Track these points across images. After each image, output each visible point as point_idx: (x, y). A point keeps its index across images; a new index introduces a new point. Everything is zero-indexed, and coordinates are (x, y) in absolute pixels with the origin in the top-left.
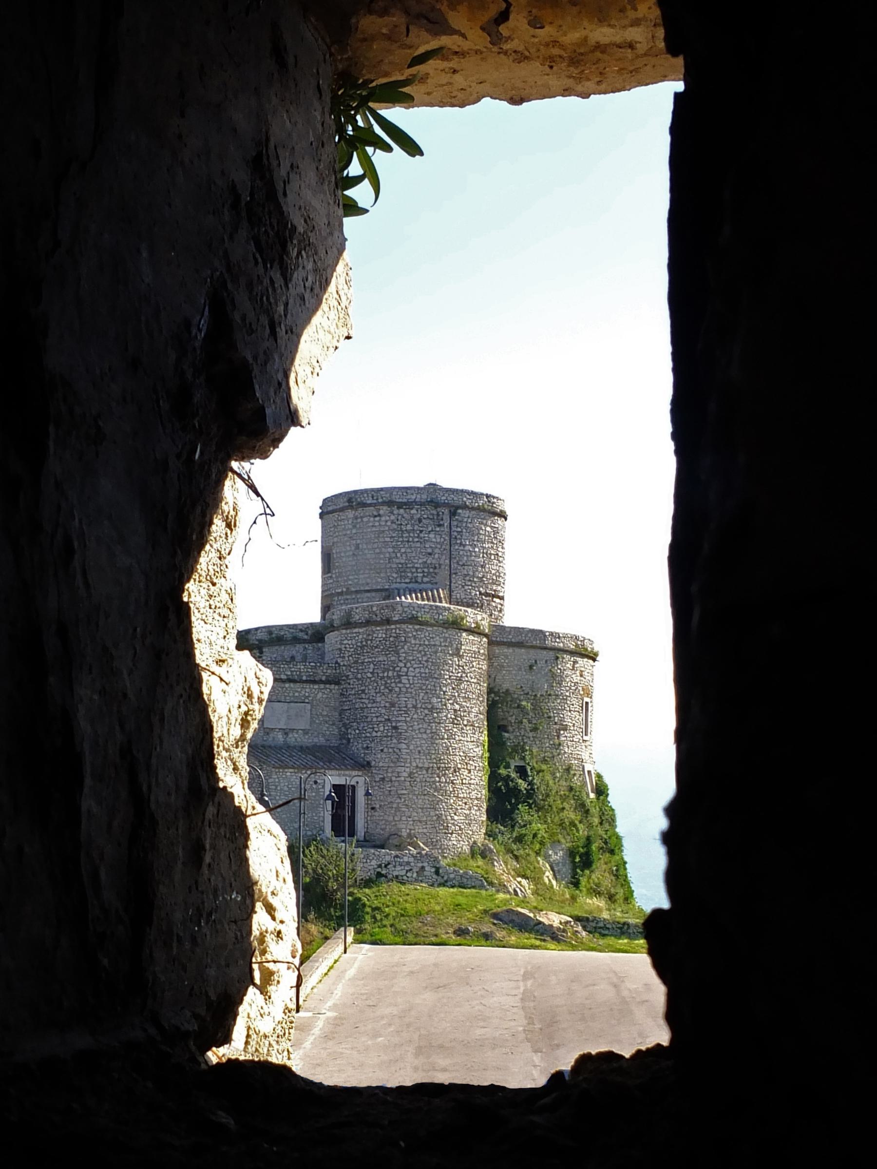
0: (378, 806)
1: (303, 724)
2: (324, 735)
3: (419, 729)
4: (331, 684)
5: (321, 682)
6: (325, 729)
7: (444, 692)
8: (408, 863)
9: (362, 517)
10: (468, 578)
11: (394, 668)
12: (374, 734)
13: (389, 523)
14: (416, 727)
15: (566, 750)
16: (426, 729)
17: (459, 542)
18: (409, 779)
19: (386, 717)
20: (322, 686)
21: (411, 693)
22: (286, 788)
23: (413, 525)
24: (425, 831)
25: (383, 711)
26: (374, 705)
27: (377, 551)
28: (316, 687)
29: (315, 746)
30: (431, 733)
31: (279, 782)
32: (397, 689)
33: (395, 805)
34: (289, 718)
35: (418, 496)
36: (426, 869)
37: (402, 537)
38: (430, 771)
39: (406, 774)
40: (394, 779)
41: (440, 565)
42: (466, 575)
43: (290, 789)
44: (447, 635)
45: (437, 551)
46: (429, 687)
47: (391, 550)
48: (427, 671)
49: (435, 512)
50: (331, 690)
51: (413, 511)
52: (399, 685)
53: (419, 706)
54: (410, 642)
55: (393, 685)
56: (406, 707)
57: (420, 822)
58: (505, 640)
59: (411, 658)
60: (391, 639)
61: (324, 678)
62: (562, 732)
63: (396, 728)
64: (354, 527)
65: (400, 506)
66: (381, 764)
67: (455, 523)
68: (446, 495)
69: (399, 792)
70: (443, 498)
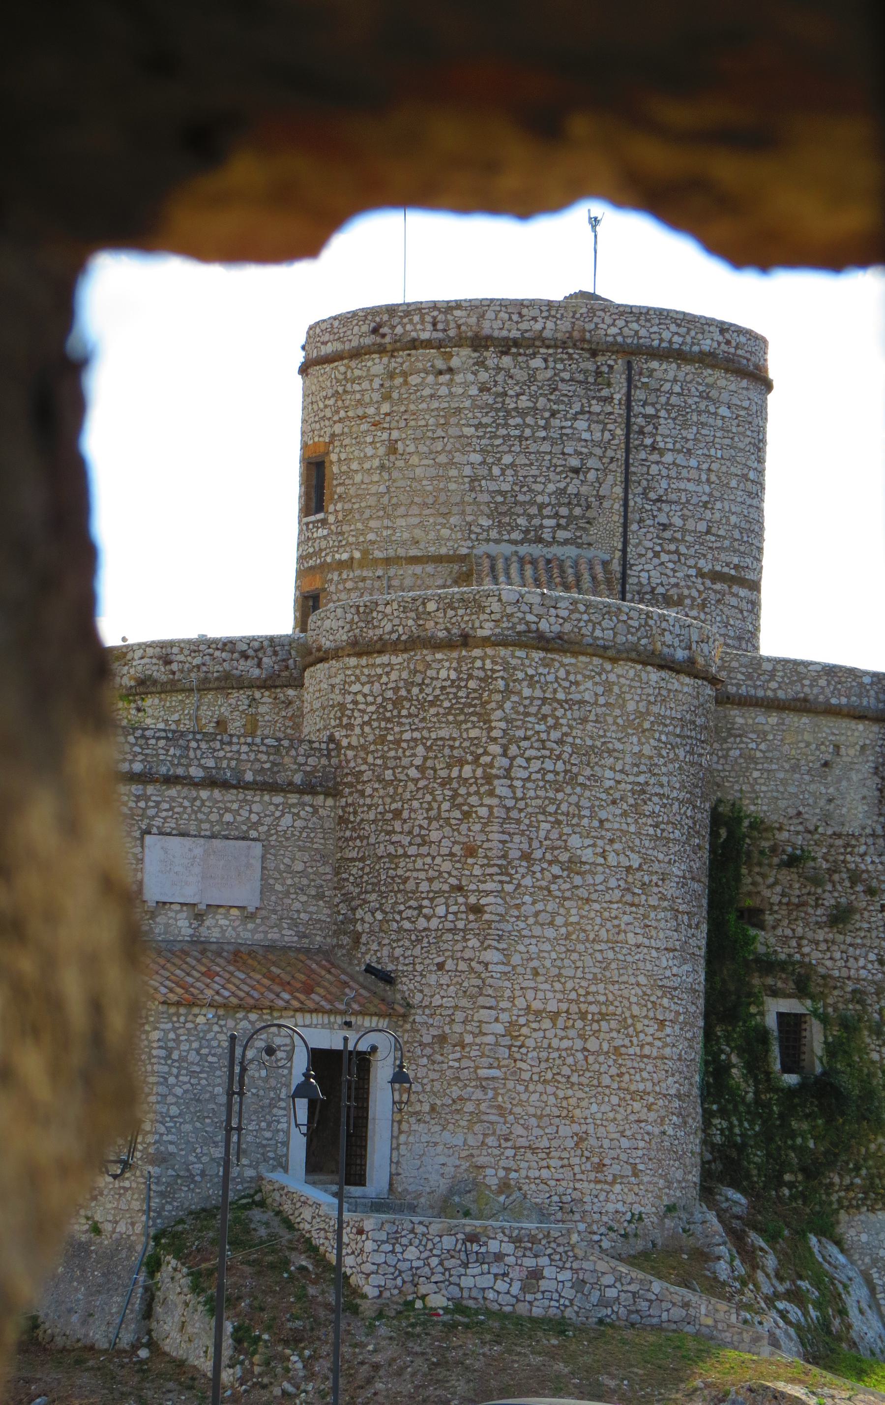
0: (426, 1108)
1: (246, 893)
2: (294, 924)
3: (537, 914)
4: (314, 793)
5: (288, 788)
6: (297, 905)
7: (601, 822)
8: (499, 1257)
9: (405, 374)
10: (667, 534)
11: (477, 758)
12: (422, 923)
13: (473, 391)
14: (528, 909)
17: (648, 441)
18: (506, 1041)
19: (453, 881)
20: (293, 799)
21: (518, 822)
22: (193, 1057)
23: (534, 397)
24: (545, 1173)
25: (447, 866)
26: (424, 850)
27: (442, 459)
28: (278, 799)
29: (271, 948)
30: (566, 924)
31: (177, 1040)
32: (483, 812)
33: (470, 1107)
35: (550, 325)
36: (546, 1273)
37: (506, 425)
38: (560, 1023)
39: (499, 1028)
40: (468, 1039)
41: (600, 498)
42: (665, 527)
43: (203, 1058)
44: (612, 678)
45: (591, 463)
47: (476, 458)
48: (560, 766)
49: (590, 366)
50: (316, 811)
52: (487, 801)
53: (538, 854)
54: (519, 693)
55: (473, 800)
56: (504, 857)
57: (534, 1150)
58: (760, 693)
59: (521, 733)
60: (472, 684)
61: (298, 779)
63: (477, 910)
64: (386, 397)
66: (437, 1001)
68: (620, 323)
69: (482, 1073)
70: (613, 331)
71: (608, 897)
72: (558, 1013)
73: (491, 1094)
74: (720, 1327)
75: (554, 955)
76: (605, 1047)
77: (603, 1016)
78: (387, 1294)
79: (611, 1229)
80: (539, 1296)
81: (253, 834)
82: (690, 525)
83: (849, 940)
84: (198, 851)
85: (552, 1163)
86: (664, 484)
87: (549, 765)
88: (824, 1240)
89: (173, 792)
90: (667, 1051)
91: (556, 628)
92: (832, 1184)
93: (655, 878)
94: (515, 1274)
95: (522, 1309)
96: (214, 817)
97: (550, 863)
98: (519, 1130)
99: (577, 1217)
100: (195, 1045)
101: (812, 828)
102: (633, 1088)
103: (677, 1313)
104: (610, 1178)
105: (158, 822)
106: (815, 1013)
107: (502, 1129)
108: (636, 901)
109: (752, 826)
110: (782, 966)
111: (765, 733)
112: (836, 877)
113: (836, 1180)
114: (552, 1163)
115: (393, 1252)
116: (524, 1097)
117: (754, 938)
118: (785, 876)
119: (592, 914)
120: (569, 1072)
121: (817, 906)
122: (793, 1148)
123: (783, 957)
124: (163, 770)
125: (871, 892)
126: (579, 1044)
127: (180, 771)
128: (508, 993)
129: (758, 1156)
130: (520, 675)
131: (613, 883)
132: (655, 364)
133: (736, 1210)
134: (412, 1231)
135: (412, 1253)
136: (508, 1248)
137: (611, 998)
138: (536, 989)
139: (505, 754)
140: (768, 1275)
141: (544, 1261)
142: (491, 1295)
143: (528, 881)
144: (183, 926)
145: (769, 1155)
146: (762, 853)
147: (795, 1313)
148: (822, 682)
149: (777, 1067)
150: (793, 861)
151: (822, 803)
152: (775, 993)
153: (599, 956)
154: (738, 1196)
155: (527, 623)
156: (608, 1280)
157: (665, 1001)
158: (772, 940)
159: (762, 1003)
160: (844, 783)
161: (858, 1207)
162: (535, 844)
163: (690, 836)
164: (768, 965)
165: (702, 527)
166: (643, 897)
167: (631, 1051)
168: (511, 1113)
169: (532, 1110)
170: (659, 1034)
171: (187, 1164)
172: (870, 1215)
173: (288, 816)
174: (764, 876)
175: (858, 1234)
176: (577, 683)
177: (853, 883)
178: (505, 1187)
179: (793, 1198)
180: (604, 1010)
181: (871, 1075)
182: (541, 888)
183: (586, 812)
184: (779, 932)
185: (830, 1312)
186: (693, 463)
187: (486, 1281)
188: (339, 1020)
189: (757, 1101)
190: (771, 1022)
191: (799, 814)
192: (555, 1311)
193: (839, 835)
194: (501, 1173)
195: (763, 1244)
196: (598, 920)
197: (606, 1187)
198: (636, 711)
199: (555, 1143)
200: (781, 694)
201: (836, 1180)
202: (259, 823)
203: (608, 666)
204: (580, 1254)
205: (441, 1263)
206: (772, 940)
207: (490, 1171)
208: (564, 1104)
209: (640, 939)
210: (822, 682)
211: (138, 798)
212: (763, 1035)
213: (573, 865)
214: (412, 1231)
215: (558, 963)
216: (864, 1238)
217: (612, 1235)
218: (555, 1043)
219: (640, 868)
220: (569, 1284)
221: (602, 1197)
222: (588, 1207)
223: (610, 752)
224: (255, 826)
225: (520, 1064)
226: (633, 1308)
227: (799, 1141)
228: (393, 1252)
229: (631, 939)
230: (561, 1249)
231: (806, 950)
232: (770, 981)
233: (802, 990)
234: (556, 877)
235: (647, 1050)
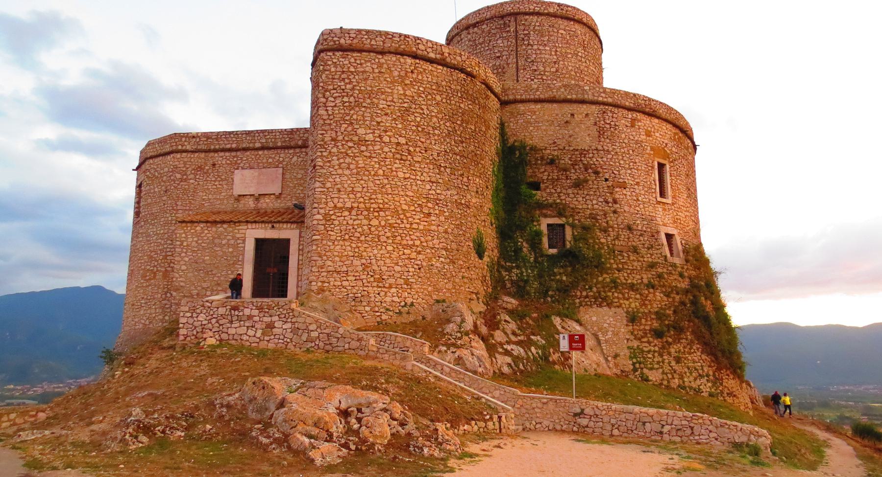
1: (276, 189)
6: (299, 191)
7: (378, 123)
8: (250, 317)
10: (537, 73)
15: (626, 208)
16: (349, 164)
17: (526, 42)
18: (323, 222)
20: (298, 150)
21: (330, 124)
22: (194, 244)
24: (345, 283)
28: (291, 151)
30: (357, 168)
31: (186, 237)
36: (276, 325)
38: (354, 212)
43: (199, 244)
44: (382, 61)
46: (355, 117)
48: (352, 99)
49: (502, 22)
51: (485, 26)
53: (340, 138)
54: (329, 70)
56: (323, 140)
58: (532, 97)
59: (331, 87)
61: (300, 143)
62: (617, 189)
65: (474, 25)
67: (522, 27)
71: (383, 156)
72: (352, 208)
73: (314, 247)
74: (381, 351)
75: (349, 182)
76: (383, 223)
77: (381, 209)
78: (188, 339)
79: (387, 309)
80: (272, 337)
81: (281, 165)
82: (548, 69)
83: (586, 193)
84: (256, 174)
85: (349, 278)
86: (534, 56)
87: (346, 99)
88: (567, 320)
89: (248, 153)
90: (433, 228)
91: (349, 42)
92: (576, 296)
93: (418, 149)
95: (263, 345)
96: (265, 161)
97: (347, 141)
98: (329, 263)
99: (364, 304)
100: (195, 239)
101: (561, 147)
102: (404, 242)
103: (354, 344)
104: (387, 285)
105: (242, 165)
106: (568, 223)
107: (320, 263)
108: (404, 158)
109: (531, 149)
110: (551, 206)
111: (535, 112)
112: (577, 167)
113: (579, 293)
114: (349, 278)
115: (192, 317)
116: (332, 247)
117: (535, 195)
118: (549, 168)
119: (373, 163)
120: (359, 235)
121: (567, 179)
122: (552, 280)
123: (550, 201)
124: (244, 146)
125: (597, 173)
126: (365, 222)
127: (251, 145)
128: (324, 200)
129: (536, 285)
130: (330, 63)
131: (386, 149)
132: (527, 17)
133: (509, 306)
134: (203, 306)
135: (202, 317)
137: (386, 201)
138: (339, 198)
139: (324, 97)
140: (506, 333)
141: (276, 318)
142: (245, 338)
143: (335, 150)
144: (251, 203)
145: (540, 284)
146: (537, 160)
147: (518, 350)
148: (562, 90)
149: (546, 246)
150: (552, 162)
151: (567, 137)
152: (546, 216)
153: (378, 182)
154: (513, 301)
155: (335, 41)
157: (430, 205)
158: (545, 195)
159: (538, 221)
160: (577, 129)
161: (591, 306)
162: (339, 134)
163: (449, 135)
164: (540, 206)
165: (553, 70)
166: (409, 157)
167: (402, 226)
168: (325, 255)
169: (336, 254)
170: (426, 219)
171: (190, 291)
172: (599, 309)
174: (539, 169)
175: (590, 317)
176: (361, 64)
177: (586, 170)
178: (321, 290)
179: (553, 302)
180: (381, 206)
181: (600, 248)
182: (342, 153)
183: (369, 119)
184: (548, 191)
185: (551, 350)
186: (547, 48)
187: (243, 330)
188: (270, 225)
189: (536, 260)
190: (544, 228)
191: (555, 143)
192: (281, 345)
193: (577, 150)
194: (320, 284)
195: (507, 318)
196: (377, 166)
197: (386, 290)
198: (399, 76)
199: (350, 269)
200: (542, 96)
201: (579, 293)
202: (283, 161)
203: (380, 57)
204: (296, 314)
205: (217, 322)
206: (545, 195)
207: (314, 283)
208: (357, 250)
209: (407, 175)
210: (562, 90)
211: (234, 157)
212: (539, 234)
213: (362, 142)
214: (203, 306)
215: (352, 185)
216: (594, 319)
217: (391, 313)
218: (350, 222)
219: (407, 144)
220: (289, 330)
221: (382, 294)
222: (372, 299)
223: (383, 93)
224: (281, 163)
225: (330, 233)
226: (328, 342)
227: (558, 277)
228: (192, 317)
229: (401, 175)
230: (285, 312)
231: (563, 198)
232: (544, 211)
233: (560, 215)
234: (350, 147)
235: (415, 226)
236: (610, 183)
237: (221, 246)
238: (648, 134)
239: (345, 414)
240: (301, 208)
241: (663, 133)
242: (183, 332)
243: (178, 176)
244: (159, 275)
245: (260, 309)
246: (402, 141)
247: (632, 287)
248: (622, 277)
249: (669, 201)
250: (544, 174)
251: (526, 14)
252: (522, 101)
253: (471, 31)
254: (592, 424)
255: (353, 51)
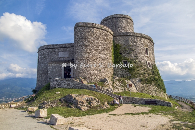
1: (67, 56)
5: (71, 47)
8: (65, 82)
15: (140, 58)
34: (64, 55)
65: (107, 20)
72: (84, 59)
94: (67, 84)
135: (55, 83)
136: (66, 81)
141: (70, 82)
143: (80, 48)
144: (63, 59)
156: (78, 84)
157: (100, 58)
173: (71, 49)
187: (64, 85)
236: (136, 52)
237: (57, 68)
238: (144, 42)
239: (87, 101)
240: (73, 59)
241: (147, 42)
242: (51, 86)
243: (47, 54)
244: (44, 74)
245: (67, 80)
246: (94, 45)
247: (141, 74)
248: (139, 72)
249: (149, 56)
250: (122, 51)
251: (117, 17)
252: (118, 36)
253: (106, 21)
254: (135, 102)
255: (83, 27)
